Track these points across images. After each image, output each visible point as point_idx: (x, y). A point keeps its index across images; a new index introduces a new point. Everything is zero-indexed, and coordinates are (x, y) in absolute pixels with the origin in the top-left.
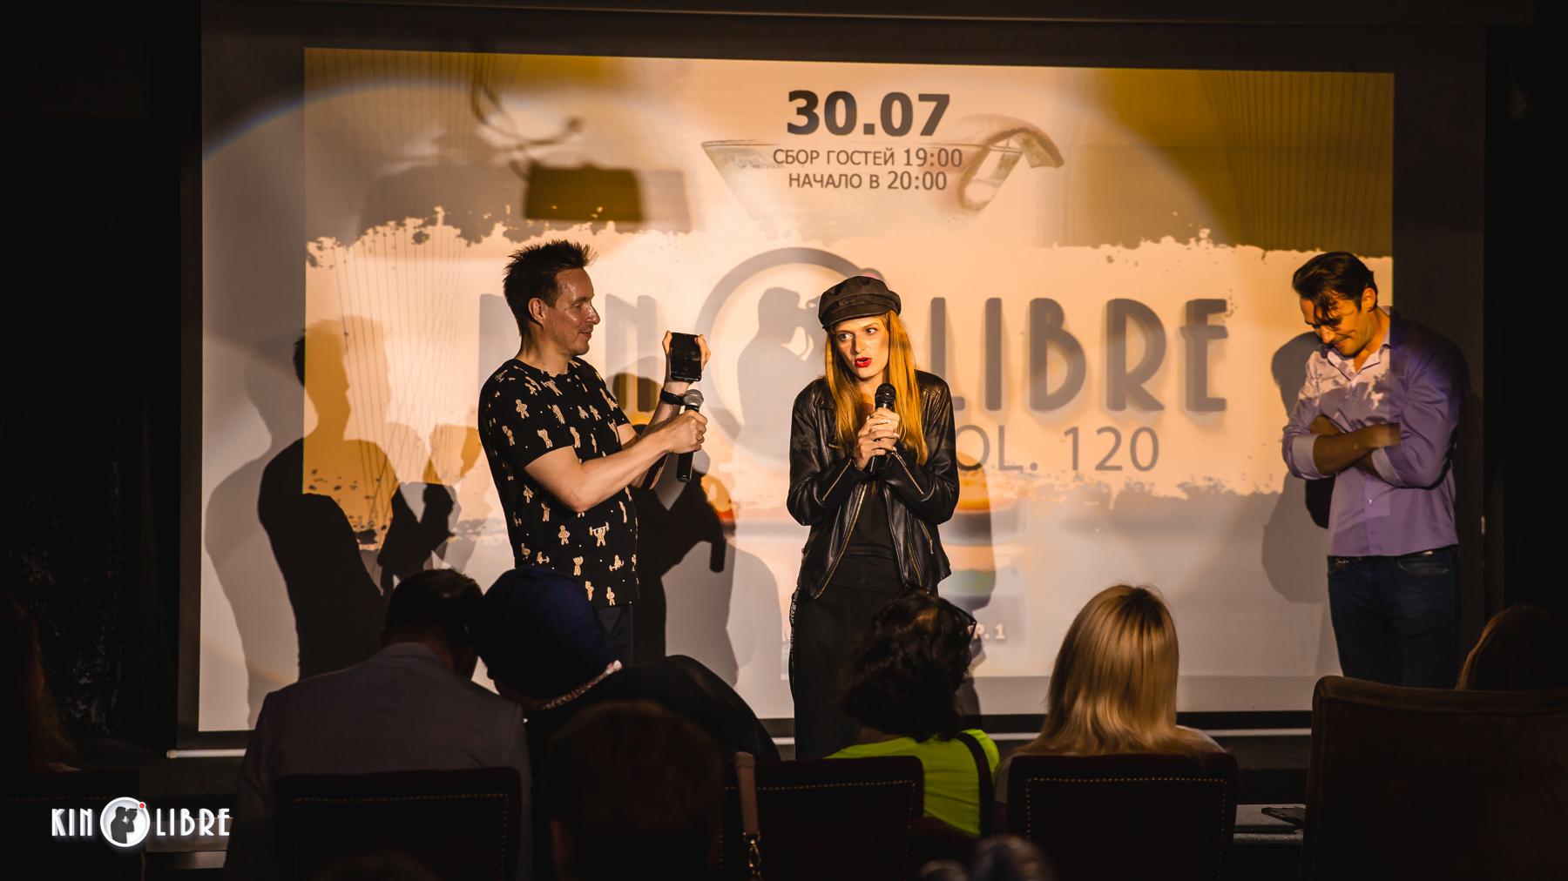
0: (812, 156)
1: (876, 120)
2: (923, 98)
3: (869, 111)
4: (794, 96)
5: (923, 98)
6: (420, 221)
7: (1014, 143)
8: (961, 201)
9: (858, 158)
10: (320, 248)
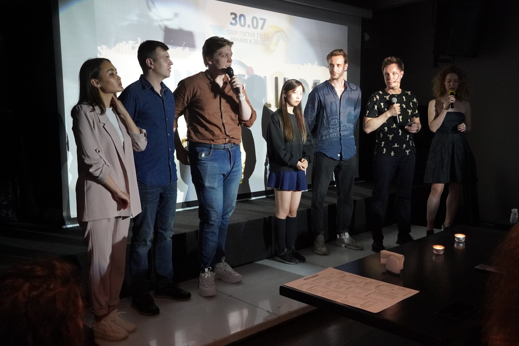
0: (236, 32)
6: (133, 42)
9: (247, 34)
10: (102, 49)
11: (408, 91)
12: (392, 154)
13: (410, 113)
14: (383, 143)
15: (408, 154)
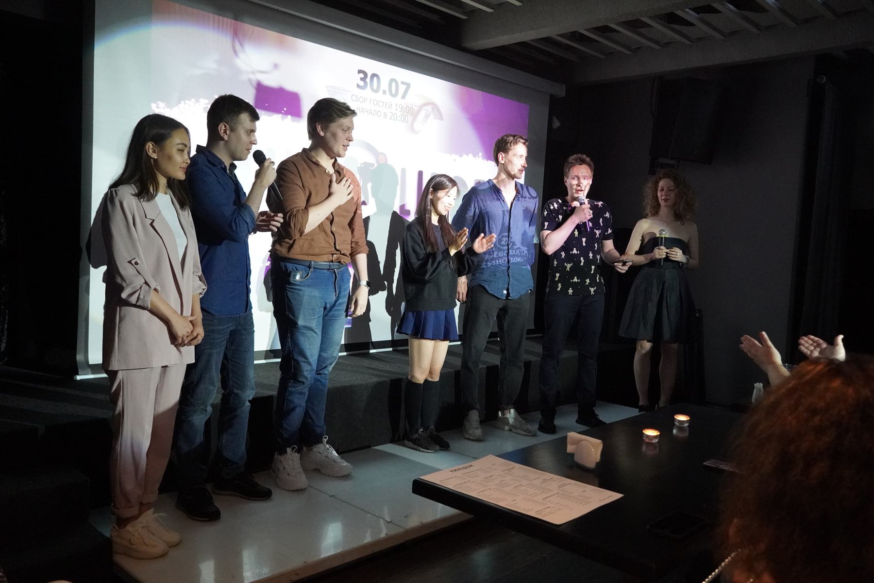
0: (365, 100)
1: (387, 89)
2: (403, 83)
3: (384, 85)
4: (360, 72)
5: (403, 83)
7: (429, 108)
8: (412, 128)
11: (599, 200)
12: (570, 291)
13: (598, 235)
14: (558, 275)
15: (592, 293)
